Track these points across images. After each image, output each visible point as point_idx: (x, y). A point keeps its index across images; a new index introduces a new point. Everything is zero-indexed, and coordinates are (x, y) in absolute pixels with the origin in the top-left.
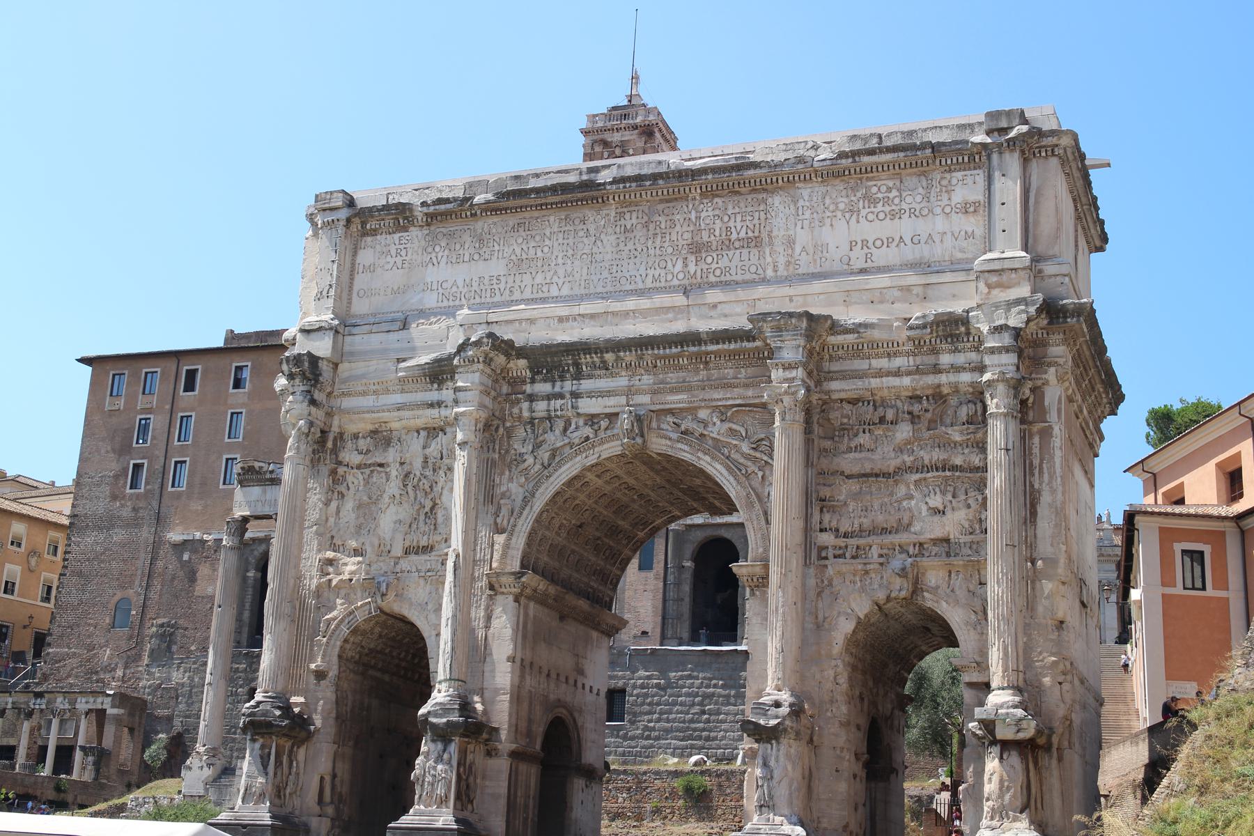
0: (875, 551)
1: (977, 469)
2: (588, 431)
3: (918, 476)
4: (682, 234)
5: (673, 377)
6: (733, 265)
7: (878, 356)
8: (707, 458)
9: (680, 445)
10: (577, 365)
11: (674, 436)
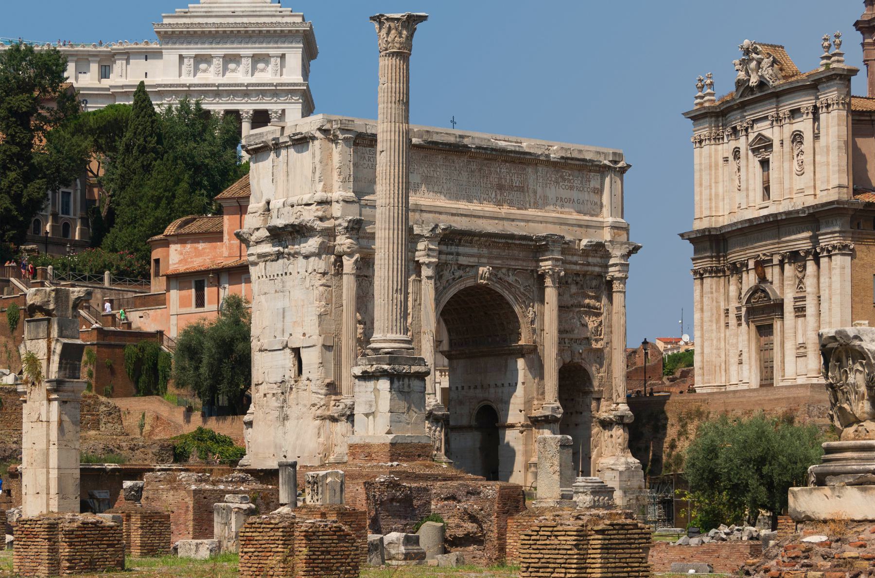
0: (566, 340)
1: (597, 309)
2: (461, 273)
3: (578, 309)
4: (493, 178)
5: (495, 252)
6: (514, 198)
7: (569, 255)
8: (507, 292)
9: (496, 285)
10: (460, 240)
11: (495, 280)
